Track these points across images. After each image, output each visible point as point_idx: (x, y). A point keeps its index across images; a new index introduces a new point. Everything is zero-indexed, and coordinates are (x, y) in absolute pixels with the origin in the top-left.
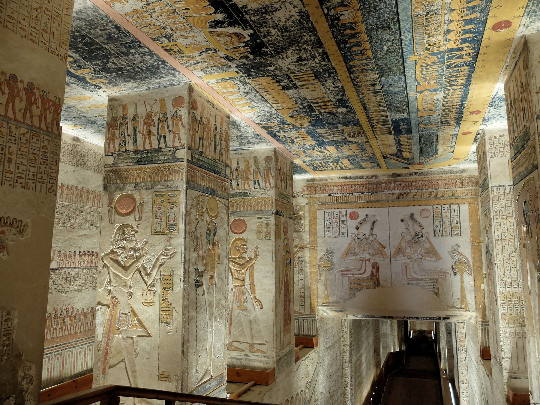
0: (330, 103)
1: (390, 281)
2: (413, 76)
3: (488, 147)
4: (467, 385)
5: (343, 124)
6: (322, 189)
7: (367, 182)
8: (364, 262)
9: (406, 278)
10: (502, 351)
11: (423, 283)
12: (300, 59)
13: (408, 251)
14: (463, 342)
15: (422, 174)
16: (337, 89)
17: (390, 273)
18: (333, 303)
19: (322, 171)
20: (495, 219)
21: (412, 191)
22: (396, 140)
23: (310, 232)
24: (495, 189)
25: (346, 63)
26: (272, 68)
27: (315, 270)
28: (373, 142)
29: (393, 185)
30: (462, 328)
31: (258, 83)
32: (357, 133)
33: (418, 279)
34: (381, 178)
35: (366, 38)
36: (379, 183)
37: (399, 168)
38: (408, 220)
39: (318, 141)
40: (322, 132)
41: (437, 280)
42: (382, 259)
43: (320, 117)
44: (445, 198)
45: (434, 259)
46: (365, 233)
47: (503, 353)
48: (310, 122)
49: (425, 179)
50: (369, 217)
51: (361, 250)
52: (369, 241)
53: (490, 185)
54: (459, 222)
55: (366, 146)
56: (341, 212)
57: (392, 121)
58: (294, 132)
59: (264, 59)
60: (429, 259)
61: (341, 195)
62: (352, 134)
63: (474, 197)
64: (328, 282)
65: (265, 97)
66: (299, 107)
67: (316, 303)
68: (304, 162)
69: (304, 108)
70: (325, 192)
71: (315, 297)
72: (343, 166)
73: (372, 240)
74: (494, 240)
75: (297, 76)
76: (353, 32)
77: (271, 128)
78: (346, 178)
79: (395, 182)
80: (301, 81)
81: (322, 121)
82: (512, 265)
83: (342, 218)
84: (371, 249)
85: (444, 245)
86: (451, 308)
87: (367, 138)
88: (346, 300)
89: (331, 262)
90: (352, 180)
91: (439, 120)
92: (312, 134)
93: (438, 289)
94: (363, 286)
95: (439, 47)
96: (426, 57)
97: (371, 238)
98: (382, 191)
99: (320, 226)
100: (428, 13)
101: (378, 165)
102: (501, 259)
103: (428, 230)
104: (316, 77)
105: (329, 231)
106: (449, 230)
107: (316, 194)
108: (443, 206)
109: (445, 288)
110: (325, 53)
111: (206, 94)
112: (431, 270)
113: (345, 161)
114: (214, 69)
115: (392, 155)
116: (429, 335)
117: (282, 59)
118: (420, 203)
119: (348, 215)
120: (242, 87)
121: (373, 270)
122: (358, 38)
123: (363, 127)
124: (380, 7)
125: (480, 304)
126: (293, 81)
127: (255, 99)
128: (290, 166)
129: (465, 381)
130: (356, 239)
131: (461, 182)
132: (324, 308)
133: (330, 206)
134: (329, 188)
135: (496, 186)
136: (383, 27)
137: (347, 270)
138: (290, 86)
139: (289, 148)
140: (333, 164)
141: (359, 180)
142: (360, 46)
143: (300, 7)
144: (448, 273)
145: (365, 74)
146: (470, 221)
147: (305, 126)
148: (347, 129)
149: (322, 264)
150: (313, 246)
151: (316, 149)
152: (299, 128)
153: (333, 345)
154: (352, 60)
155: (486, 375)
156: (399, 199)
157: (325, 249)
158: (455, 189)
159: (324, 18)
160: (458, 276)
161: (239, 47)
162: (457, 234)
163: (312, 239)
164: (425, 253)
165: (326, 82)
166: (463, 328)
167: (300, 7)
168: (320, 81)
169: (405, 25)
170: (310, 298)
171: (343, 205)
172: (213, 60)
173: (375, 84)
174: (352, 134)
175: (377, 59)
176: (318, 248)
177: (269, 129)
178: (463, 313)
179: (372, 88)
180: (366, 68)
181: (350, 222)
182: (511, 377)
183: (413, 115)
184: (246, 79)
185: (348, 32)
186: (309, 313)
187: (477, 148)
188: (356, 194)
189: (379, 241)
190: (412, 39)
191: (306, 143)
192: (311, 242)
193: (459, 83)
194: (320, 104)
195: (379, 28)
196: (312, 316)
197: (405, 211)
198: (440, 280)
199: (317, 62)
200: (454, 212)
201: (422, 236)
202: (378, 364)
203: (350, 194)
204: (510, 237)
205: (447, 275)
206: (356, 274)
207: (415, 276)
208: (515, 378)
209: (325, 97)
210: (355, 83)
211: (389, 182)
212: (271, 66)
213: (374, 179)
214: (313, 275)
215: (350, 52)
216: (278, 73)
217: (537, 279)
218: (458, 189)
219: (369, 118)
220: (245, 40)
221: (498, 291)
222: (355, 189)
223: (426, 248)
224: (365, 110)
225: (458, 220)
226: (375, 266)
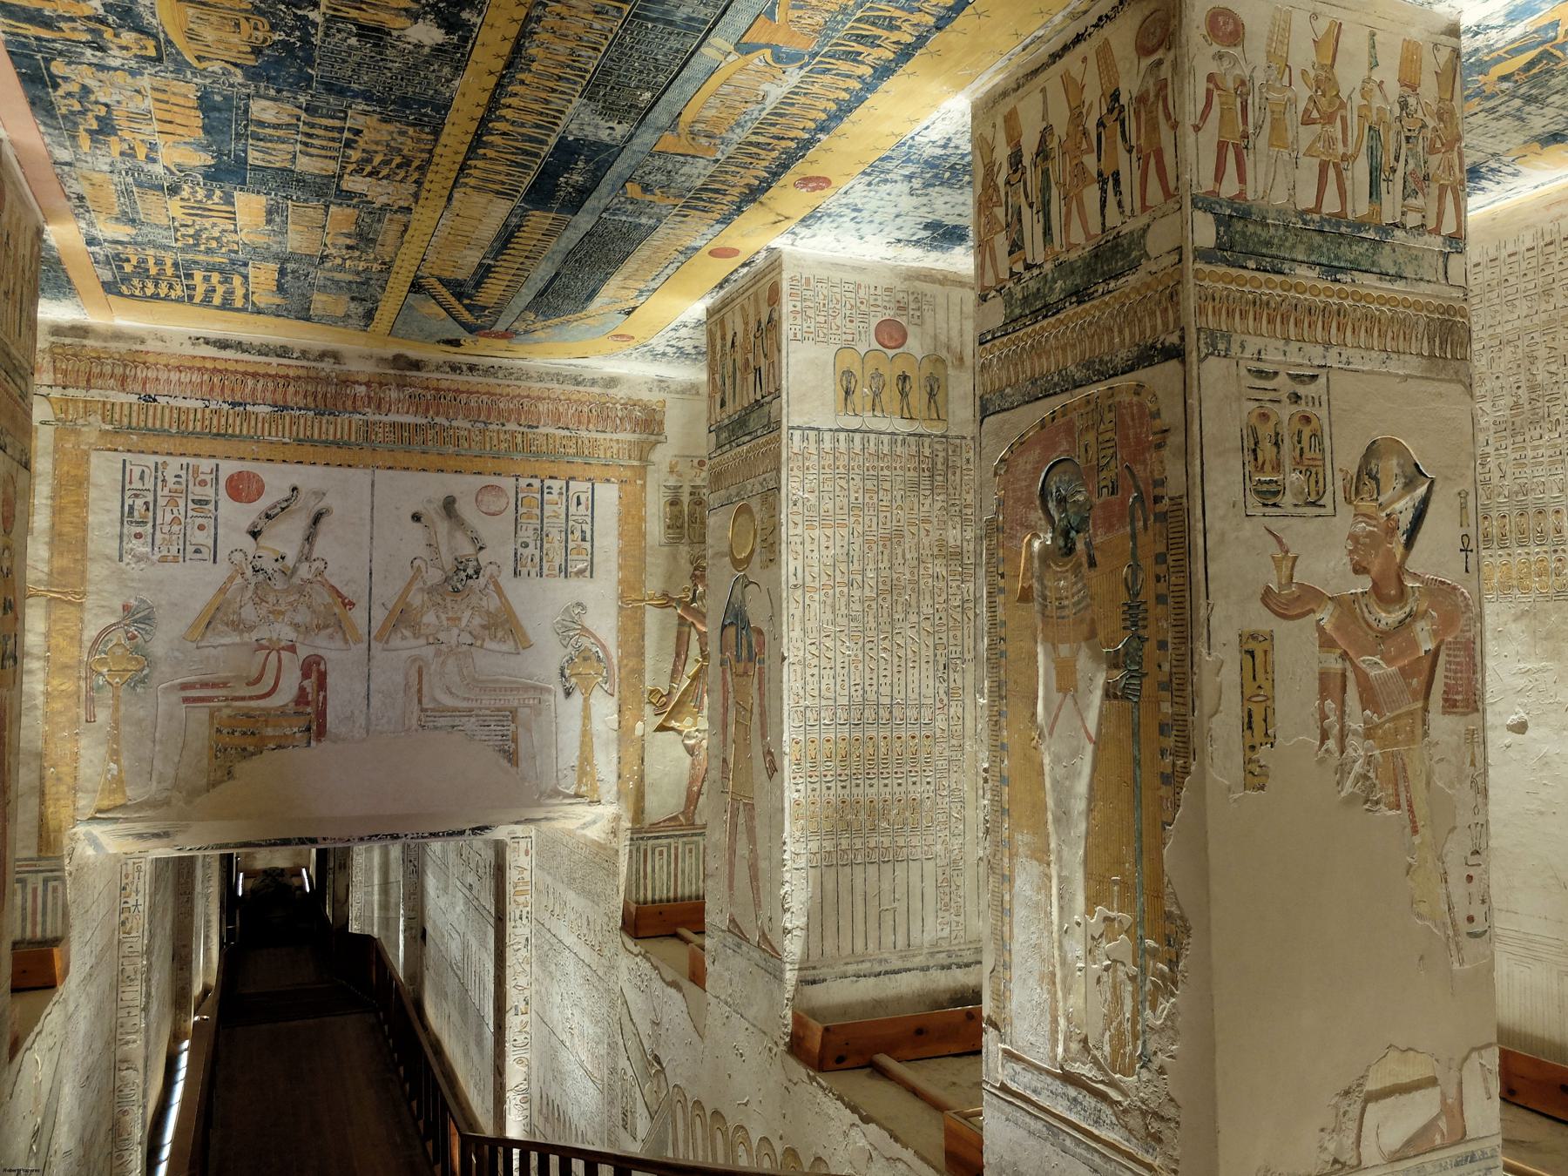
1: (362, 721)
3: (787, 306)
4: (525, 1018)
6: (119, 371)
7: (302, 373)
8: (274, 655)
9: (416, 708)
10: (785, 911)
11: (470, 724)
13: (430, 618)
14: (523, 893)
15: (490, 371)
17: (364, 692)
18: (140, 806)
19: (145, 298)
20: (791, 525)
21: (454, 423)
22: (506, 225)
23: (56, 538)
24: (797, 434)
27: (69, 686)
28: (424, 217)
29: (394, 394)
30: (522, 853)
32: (398, 160)
33: (456, 709)
34: (352, 366)
36: (346, 381)
37: (427, 338)
38: (437, 519)
39: (220, 153)
40: (268, 117)
41: (514, 713)
42: (339, 644)
43: (316, 40)
44: (554, 456)
45: (508, 646)
46: (282, 550)
47: (788, 915)
48: (257, 51)
49: (498, 391)
50: (302, 495)
51: (263, 612)
52: (296, 580)
53: (784, 421)
54: (588, 537)
55: (388, 231)
56: (196, 470)
57: (562, 139)
58: (145, 82)
60: (493, 646)
61: (200, 404)
62: (377, 159)
63: (636, 463)
64: (126, 729)
67: (65, 814)
68: (91, 241)
70: (130, 386)
71: (63, 788)
72: (240, 292)
73: (306, 576)
74: (784, 586)
77: (47, 23)
78: (223, 345)
79: (401, 387)
81: (309, 61)
82: (824, 662)
83: (198, 489)
84: (302, 609)
85: (542, 602)
86: (550, 797)
87: (416, 196)
88: (193, 794)
89: (139, 652)
90: (246, 357)
91: (699, 183)
92: (218, 114)
93: (515, 740)
94: (263, 738)
97: (304, 571)
98: (355, 411)
99: (103, 515)
101: (369, 316)
102: (800, 644)
103: (498, 554)
105: (138, 536)
106: (558, 560)
107: (89, 387)
108: (548, 482)
109: (536, 737)
112: (497, 681)
113: (263, 276)
115: (445, 283)
116: (295, 881)
118: (479, 464)
119: (222, 482)
121: (306, 683)
123: (443, 139)
125: (629, 779)
128: (33, 246)
129: (522, 1006)
130: (249, 572)
131: (603, 415)
132: (97, 830)
133: (152, 442)
134: (151, 374)
135: (799, 428)
137: (204, 685)
139: (64, 155)
140: (207, 279)
141: (275, 361)
144: (548, 691)
146: (621, 536)
147: (216, 67)
148: (375, 131)
149: (103, 662)
150: (68, 591)
151: (185, 194)
152: (181, 66)
153: (100, 959)
155: (657, 985)
156: (410, 446)
157: (118, 604)
158: (584, 434)
160: (577, 698)
162: (581, 572)
163: (63, 562)
164: (484, 627)
166: (527, 853)
170: (42, 794)
171: (206, 445)
174: (377, 159)
176: (89, 601)
177: (32, 30)
178: (580, 809)
181: (227, 507)
182: (804, 982)
183: (645, 138)
186: (33, 853)
187: (711, 312)
188: (257, 409)
189: (333, 581)
191: (162, 150)
192: (56, 577)
193: (876, 53)
196: (44, 865)
197: (428, 488)
198: (524, 713)
200: (579, 503)
201: (477, 572)
202: (180, 999)
203: (234, 404)
204: (824, 578)
205: (546, 696)
206: (243, 699)
207: (448, 701)
208: (814, 982)
211: (381, 384)
213: (327, 366)
214: (58, 706)
217: (1098, 695)
218: (594, 435)
219: (494, 104)
221: (785, 737)
222: (254, 390)
223: (488, 613)
224: (509, 65)
225: (587, 528)
226: (314, 670)
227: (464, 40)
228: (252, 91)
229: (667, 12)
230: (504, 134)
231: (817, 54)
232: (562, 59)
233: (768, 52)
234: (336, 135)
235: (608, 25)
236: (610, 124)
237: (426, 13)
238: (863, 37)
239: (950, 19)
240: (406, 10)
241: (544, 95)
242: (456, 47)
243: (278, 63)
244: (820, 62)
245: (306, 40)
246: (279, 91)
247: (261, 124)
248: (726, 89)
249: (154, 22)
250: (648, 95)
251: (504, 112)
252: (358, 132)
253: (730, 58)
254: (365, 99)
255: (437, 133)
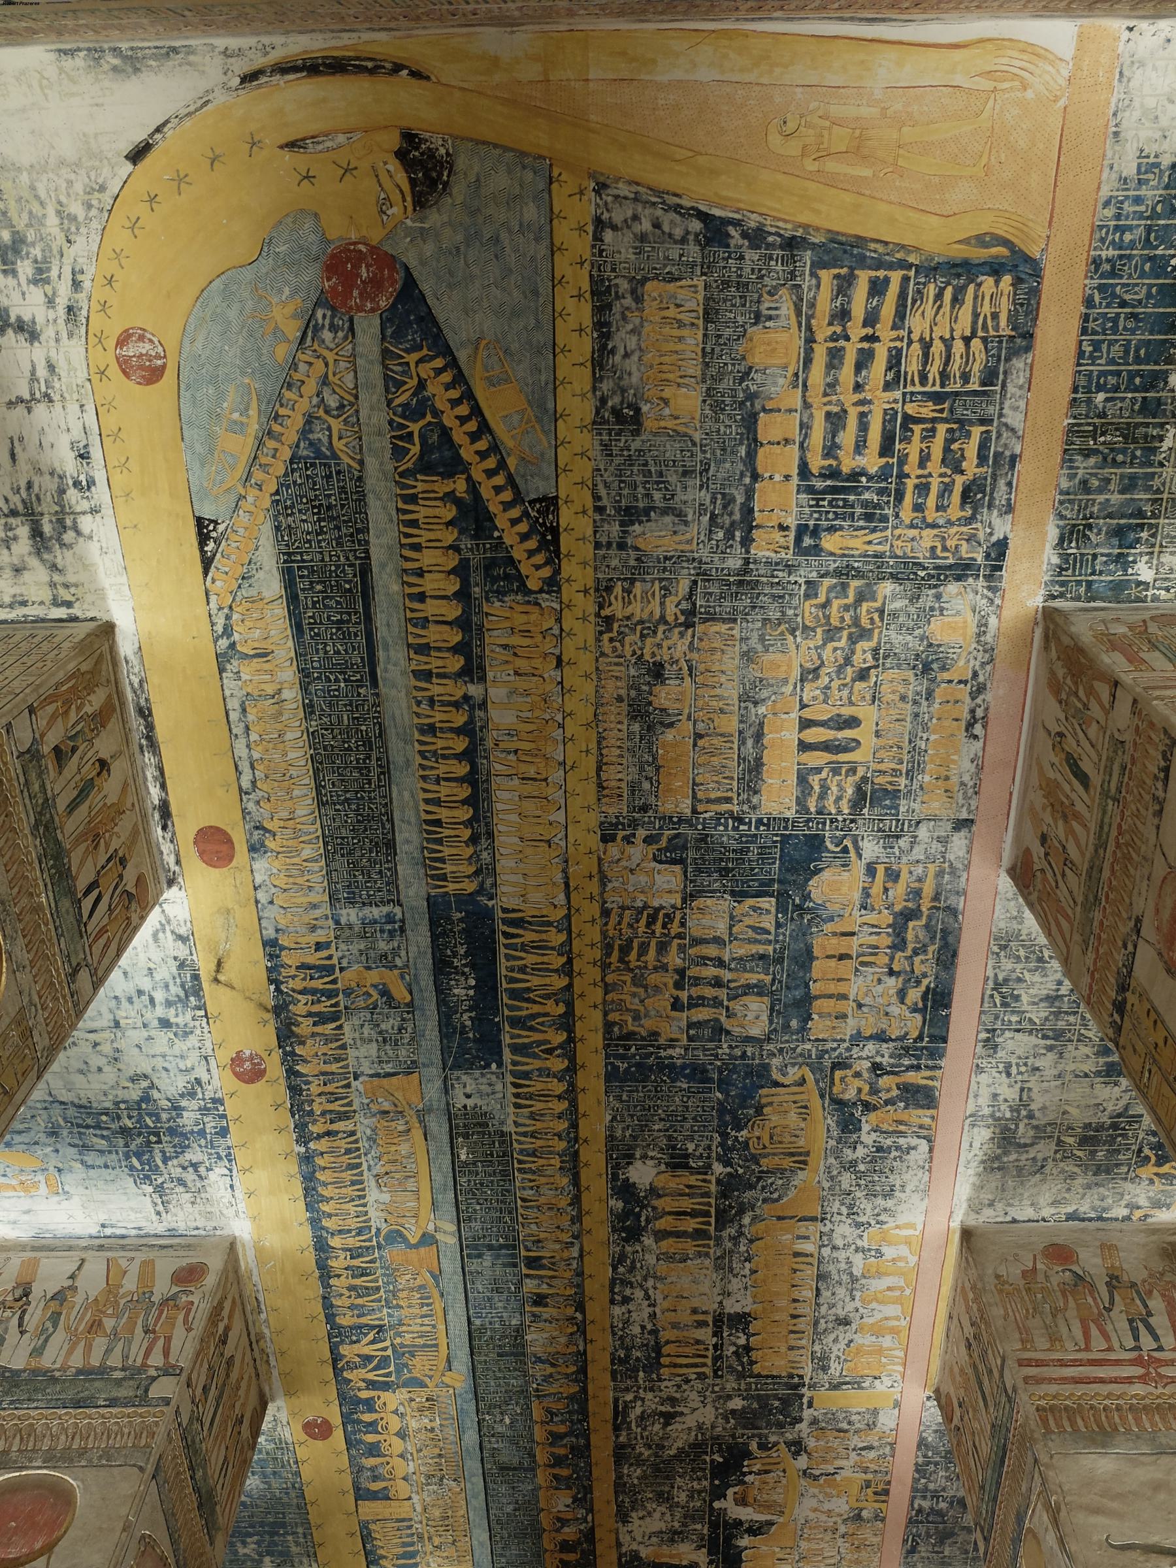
0: (662, 1224)
2: (450, 1317)
5: (661, 1067)
12: (668, 1418)
16: (628, 1292)
25: (584, 1390)
26: (737, 1404)
31: (792, 1355)
35: (538, 1451)
43: (717, 1138)
59: (733, 1436)
65: (809, 1294)
66: (754, 1219)
69: (741, 1211)
75: (695, 1365)
76: (557, 1471)
80: (698, 1342)
81: (722, 1110)
95: (412, 1400)
96: (431, 1377)
100: (441, 1479)
104: (658, 1348)
110: (617, 1429)
111: (937, 1343)
114: (849, 1423)
117: (700, 1427)
120: (837, 1350)
122: (552, 1454)
123: (597, 1017)
124: (511, 1507)
126: (715, 1346)
127: (841, 1292)
136: (508, 1469)
138: (730, 1328)
142: (551, 1433)
143: (623, 1530)
145: (551, 1350)
154: (571, 1398)
159: (596, 1508)
161: (759, 1473)
165: (643, 1327)
167: (623, 1530)
168: (654, 1332)
169: (473, 1465)
172: (829, 1449)
173: (536, 1303)
175: (523, 1392)
179: (544, 1289)
180: (550, 1370)
183: (433, 1090)
184: (807, 1380)
185: (565, 1472)
190: (461, 1431)
194: (691, 1224)
195: (515, 1469)
199: (639, 1403)
209: (669, 1257)
210: (578, 1315)
212: (733, 1412)
215: (572, 1421)
216: (731, 1384)
220: (736, 1489)
224: (576, 1153)
227: (615, 1177)
228: (767, 1047)
229: (498, 1257)
230: (549, 1052)
231: (379, 1247)
232: (543, 1180)
233: (413, 1241)
234: (695, 991)
235: (527, 1231)
236: (470, 1103)
237: (645, 1197)
238: (362, 1275)
239: (325, 1307)
240: (659, 1196)
241: (539, 1125)
242: (617, 1166)
243: (746, 1097)
244: (370, 1240)
245: (724, 1135)
246: (744, 1055)
247: (758, 990)
248: (411, 1185)
249: (829, 1121)
250: (463, 1157)
251: (560, 1088)
252: (676, 1005)
253: (431, 1227)
254: (672, 1067)
255: (608, 1026)
